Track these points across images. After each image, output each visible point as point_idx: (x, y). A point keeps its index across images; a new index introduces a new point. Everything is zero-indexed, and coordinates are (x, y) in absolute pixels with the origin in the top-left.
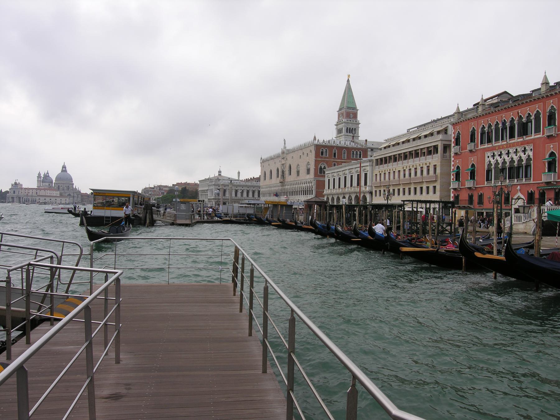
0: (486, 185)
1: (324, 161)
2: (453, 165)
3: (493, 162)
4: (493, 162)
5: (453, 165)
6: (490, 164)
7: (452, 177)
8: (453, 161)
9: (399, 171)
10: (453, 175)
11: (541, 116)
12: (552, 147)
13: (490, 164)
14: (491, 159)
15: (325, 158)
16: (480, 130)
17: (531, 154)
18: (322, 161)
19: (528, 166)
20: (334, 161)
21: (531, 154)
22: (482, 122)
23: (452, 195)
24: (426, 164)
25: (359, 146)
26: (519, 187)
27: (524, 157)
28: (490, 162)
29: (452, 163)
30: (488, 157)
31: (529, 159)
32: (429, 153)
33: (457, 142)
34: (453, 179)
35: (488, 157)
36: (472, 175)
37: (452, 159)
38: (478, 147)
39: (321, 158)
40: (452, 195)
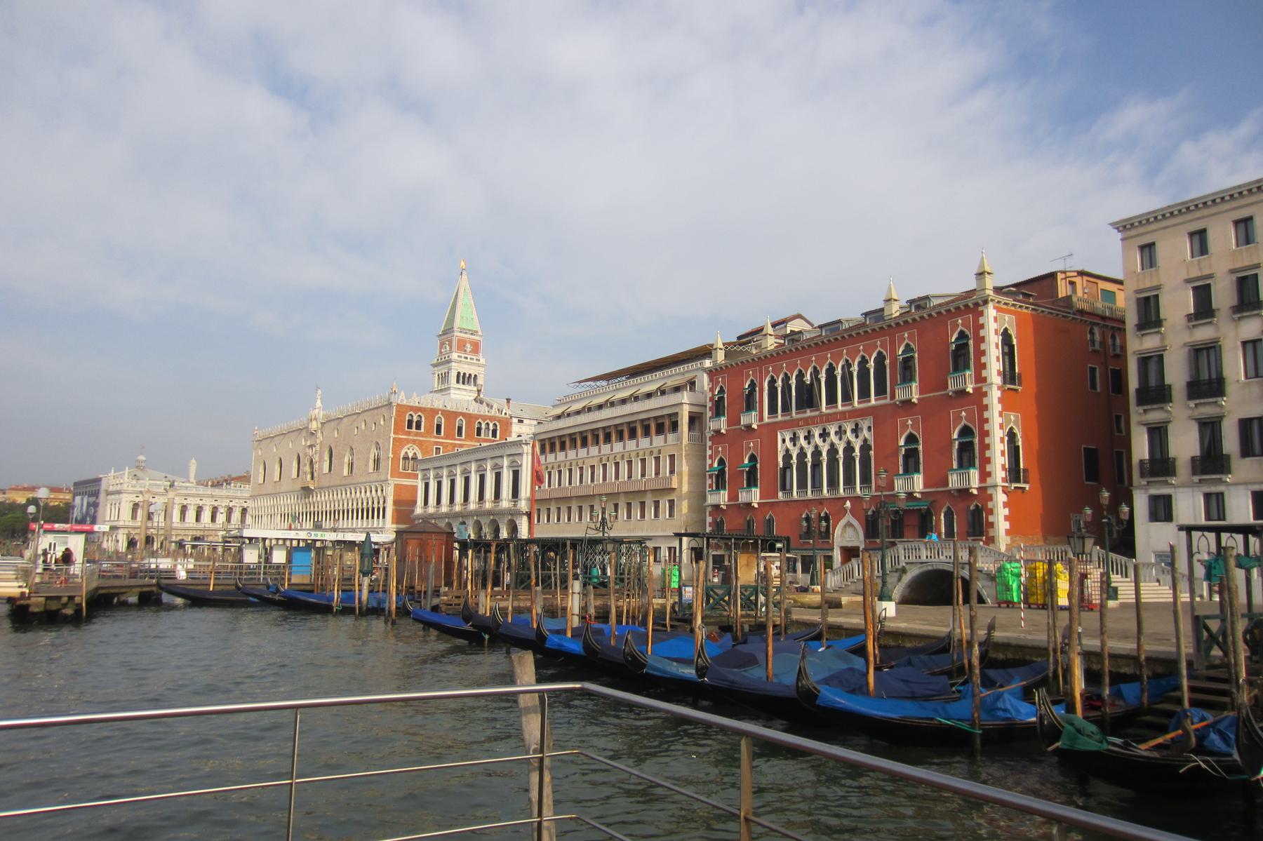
1: (414, 442)
2: (711, 457)
5: (711, 457)
6: (788, 456)
7: (709, 482)
8: (711, 448)
9: (593, 467)
10: (711, 476)
11: (887, 362)
12: (910, 424)
13: (788, 456)
14: (789, 444)
15: (417, 435)
18: (408, 441)
20: (437, 443)
23: (709, 519)
24: (651, 453)
25: (493, 413)
26: (848, 504)
28: (787, 450)
29: (709, 452)
30: (784, 441)
31: (865, 447)
32: (660, 430)
33: (718, 410)
34: (711, 486)
35: (784, 441)
37: (709, 443)
38: (761, 419)
39: (409, 433)
40: (709, 519)
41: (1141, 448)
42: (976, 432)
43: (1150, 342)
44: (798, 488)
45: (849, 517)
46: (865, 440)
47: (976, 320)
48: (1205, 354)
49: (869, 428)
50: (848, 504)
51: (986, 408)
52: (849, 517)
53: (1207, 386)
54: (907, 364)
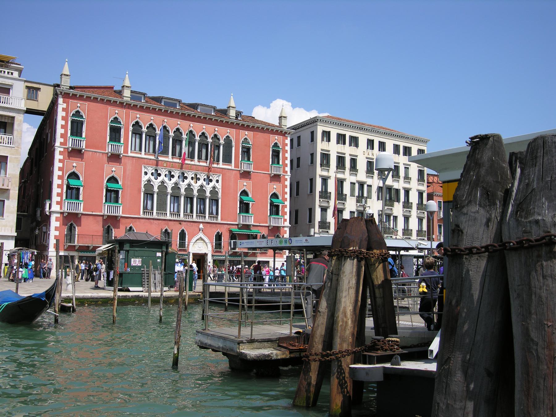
0: (142, 216)
2: (60, 169)
3: (156, 183)
4: (156, 183)
5: (60, 169)
8: (60, 161)
11: (233, 144)
12: (245, 184)
16: (131, 128)
17: (219, 186)
19: (215, 200)
21: (219, 186)
22: (138, 116)
27: (208, 188)
29: (57, 165)
31: (214, 191)
35: (146, 173)
36: (113, 195)
37: (58, 157)
38: (126, 151)
41: (318, 217)
42: (280, 198)
43: (325, 173)
44: (157, 210)
45: (201, 235)
46: (214, 188)
47: (284, 141)
48: (340, 183)
49: (217, 181)
50: (201, 226)
51: (286, 186)
52: (201, 235)
53: (341, 196)
54: (246, 151)
